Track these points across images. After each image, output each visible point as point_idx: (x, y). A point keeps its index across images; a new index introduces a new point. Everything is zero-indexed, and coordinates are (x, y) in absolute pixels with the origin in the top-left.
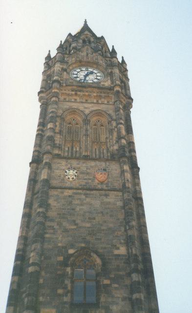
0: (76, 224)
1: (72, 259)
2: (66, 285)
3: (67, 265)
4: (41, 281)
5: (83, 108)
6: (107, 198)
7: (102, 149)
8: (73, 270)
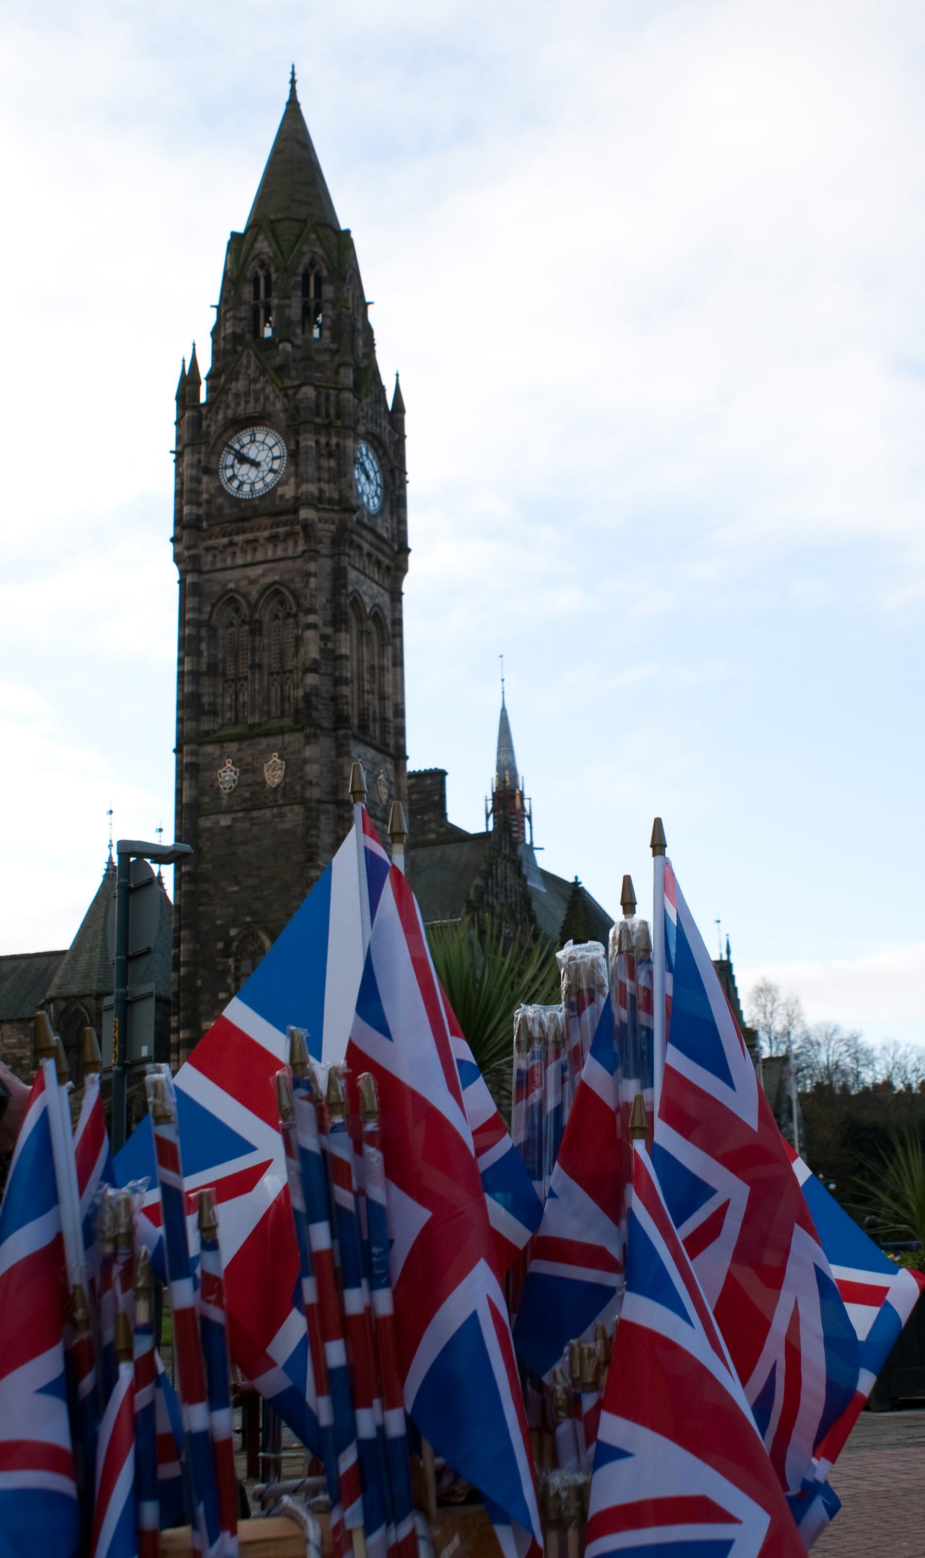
1: (235, 944)
2: (229, 985)
3: (228, 957)
4: (199, 983)
5: (246, 582)
6: (282, 821)
7: (287, 687)
8: (237, 961)
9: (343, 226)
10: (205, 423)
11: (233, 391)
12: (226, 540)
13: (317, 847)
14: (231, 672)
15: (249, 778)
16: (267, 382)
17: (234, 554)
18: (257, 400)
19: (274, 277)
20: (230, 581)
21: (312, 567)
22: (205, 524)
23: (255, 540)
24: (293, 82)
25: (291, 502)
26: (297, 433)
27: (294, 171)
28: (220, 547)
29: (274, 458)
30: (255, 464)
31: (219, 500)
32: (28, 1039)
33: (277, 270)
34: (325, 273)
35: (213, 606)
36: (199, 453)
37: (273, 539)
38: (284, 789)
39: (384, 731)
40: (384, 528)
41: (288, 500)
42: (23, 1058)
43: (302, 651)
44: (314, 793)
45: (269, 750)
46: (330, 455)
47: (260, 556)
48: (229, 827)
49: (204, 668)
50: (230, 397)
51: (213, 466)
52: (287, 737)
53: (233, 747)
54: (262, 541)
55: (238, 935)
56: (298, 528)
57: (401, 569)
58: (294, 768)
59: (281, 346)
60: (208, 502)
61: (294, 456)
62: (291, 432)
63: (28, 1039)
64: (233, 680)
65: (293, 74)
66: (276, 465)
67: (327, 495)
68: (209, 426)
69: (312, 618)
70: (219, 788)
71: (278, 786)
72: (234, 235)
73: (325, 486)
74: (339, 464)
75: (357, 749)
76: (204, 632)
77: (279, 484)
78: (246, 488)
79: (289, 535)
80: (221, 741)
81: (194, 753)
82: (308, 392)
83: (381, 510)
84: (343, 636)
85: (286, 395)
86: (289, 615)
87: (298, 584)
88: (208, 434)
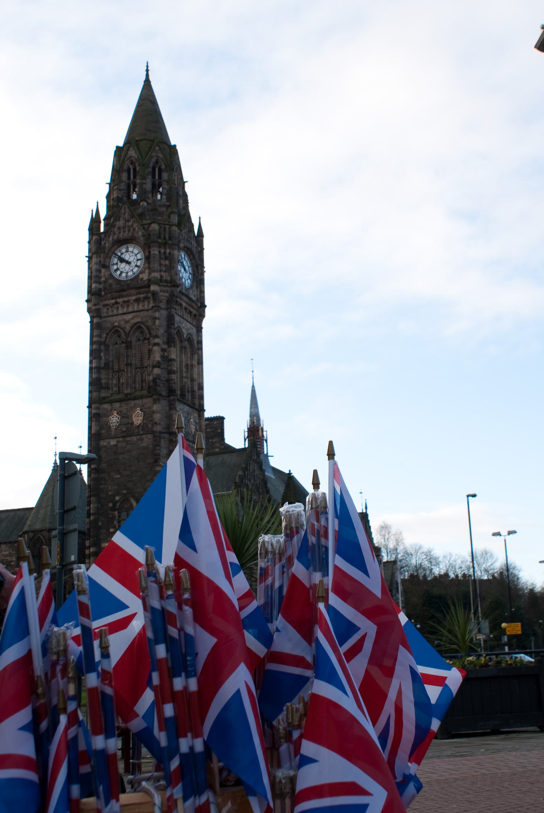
0: (120, 474)
1: (118, 504)
2: (115, 525)
3: (115, 510)
4: (100, 524)
6: (142, 442)
7: (144, 375)
8: (119, 513)
9: (173, 143)
10: (103, 242)
11: (117, 226)
12: (113, 301)
13: (159, 455)
14: (116, 367)
15: (125, 420)
16: (134, 221)
17: (118, 308)
18: (129, 231)
19: (138, 169)
20: (116, 322)
21: (157, 314)
22: (103, 293)
23: (128, 301)
24: (147, 71)
25: (146, 282)
26: (150, 247)
27: (147, 116)
28: (111, 305)
29: (138, 260)
30: (128, 263)
31: (110, 281)
32: (14, 552)
33: (139, 165)
34: (163, 167)
35: (107, 334)
36: (100, 257)
37: (137, 300)
38: (143, 426)
39: (193, 397)
40: (193, 295)
41: (145, 281)
42: (11, 561)
43: (152, 356)
44: (158, 428)
45: (135, 406)
46: (166, 258)
47: (130, 309)
48: (115, 445)
49: (102, 365)
50: (116, 229)
51: (107, 264)
52: (145, 400)
53: (117, 405)
54: (131, 301)
55: (120, 499)
56: (150, 295)
57: (202, 315)
58: (148, 416)
59: (141, 204)
60: (105, 282)
61: (148, 259)
62: (146, 247)
63: (14, 552)
64: (117, 371)
65: (147, 66)
66: (139, 263)
67: (164, 278)
68: (105, 244)
69: (157, 340)
70: (110, 426)
71: (140, 424)
72: (118, 148)
73: (163, 274)
74: (170, 263)
75: (179, 406)
76: (102, 347)
77: (141, 273)
78: (124, 275)
79: (146, 298)
80: (111, 402)
81: (98, 408)
82: (155, 226)
83: (192, 286)
84: (172, 349)
85: (144, 228)
86: (145, 339)
87: (150, 323)
88: (104, 248)
